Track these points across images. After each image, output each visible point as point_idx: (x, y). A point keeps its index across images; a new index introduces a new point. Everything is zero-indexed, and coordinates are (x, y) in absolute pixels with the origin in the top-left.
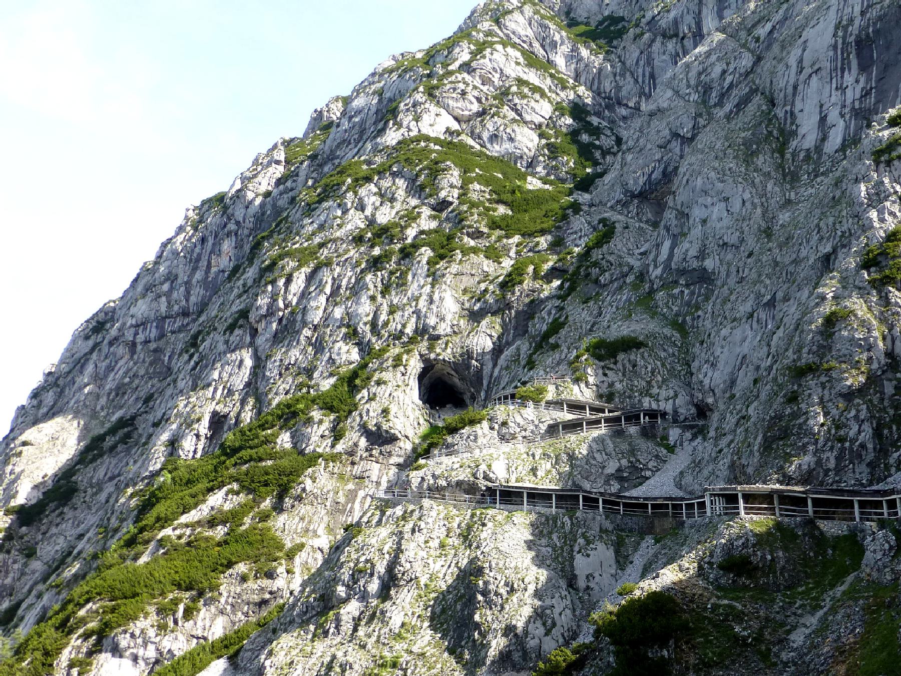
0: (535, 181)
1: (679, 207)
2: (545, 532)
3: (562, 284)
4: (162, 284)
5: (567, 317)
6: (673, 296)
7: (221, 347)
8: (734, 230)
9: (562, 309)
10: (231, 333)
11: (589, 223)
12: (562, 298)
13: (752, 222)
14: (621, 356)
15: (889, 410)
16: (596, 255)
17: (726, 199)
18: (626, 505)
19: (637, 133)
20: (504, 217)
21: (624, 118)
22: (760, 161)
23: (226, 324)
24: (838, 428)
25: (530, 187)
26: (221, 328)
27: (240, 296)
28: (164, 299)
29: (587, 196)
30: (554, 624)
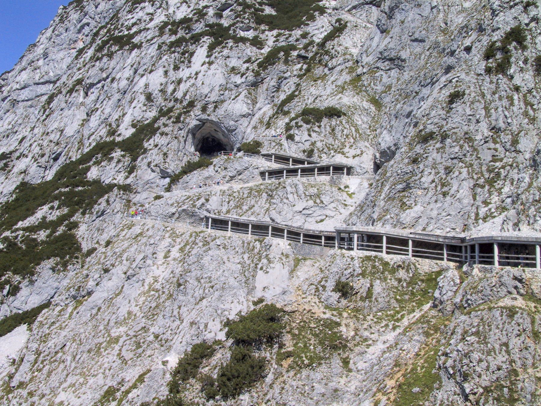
4: (38, 60)
5: (300, 91)
8: (421, 29)
10: (70, 95)
11: (329, 22)
15: (485, 173)
18: (305, 236)
20: (270, 16)
23: (68, 89)
24: (443, 185)
26: (64, 92)
27: (79, 69)
28: (38, 71)
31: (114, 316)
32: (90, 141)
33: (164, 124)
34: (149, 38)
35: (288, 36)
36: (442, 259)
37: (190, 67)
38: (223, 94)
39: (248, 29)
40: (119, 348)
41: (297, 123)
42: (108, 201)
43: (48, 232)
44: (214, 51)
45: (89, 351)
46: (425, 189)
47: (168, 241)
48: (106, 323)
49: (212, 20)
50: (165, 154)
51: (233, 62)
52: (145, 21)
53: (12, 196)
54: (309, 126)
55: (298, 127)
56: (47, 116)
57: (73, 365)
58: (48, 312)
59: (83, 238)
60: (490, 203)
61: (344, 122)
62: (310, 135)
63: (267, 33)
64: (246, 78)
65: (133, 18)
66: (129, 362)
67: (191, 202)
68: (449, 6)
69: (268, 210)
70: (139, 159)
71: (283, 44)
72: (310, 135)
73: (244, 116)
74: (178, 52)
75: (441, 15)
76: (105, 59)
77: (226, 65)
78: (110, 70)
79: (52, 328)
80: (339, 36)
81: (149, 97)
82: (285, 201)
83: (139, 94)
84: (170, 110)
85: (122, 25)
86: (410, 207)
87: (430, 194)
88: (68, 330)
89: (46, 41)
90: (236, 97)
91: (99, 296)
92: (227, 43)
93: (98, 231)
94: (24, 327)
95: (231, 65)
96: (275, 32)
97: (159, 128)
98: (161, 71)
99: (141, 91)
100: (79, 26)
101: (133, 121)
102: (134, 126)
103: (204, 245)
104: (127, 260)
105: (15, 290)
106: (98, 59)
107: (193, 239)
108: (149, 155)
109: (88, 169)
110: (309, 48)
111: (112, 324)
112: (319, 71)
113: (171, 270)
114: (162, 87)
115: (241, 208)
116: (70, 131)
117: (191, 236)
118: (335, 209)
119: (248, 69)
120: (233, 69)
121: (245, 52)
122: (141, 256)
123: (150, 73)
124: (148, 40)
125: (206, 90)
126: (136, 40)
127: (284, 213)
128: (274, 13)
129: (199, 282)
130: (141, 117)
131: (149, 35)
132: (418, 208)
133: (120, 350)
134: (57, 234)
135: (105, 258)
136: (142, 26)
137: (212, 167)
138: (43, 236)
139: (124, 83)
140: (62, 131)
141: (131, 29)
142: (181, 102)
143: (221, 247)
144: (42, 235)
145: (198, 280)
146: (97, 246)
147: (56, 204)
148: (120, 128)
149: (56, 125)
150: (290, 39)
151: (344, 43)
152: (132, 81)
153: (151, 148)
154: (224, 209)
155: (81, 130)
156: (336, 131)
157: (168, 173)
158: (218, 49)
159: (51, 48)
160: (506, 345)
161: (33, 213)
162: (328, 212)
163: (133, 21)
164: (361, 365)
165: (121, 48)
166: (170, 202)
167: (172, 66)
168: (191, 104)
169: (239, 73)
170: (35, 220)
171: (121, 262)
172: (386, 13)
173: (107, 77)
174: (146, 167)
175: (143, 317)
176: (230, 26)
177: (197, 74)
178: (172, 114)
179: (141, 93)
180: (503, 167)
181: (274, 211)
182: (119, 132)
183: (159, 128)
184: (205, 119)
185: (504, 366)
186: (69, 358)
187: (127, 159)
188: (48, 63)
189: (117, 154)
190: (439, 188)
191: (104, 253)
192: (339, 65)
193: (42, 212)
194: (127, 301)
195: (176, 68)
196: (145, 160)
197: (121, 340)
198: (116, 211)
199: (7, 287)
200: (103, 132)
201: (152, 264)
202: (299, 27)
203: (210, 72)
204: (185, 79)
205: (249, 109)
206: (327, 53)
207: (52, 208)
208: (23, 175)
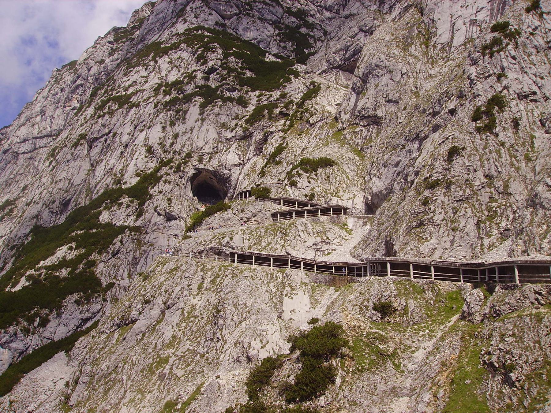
0: (270, 57)
1: (361, 76)
2: (265, 282)
3: (285, 122)
5: (287, 144)
6: (355, 133)
7: (69, 157)
8: (395, 92)
9: (285, 138)
10: (76, 148)
11: (304, 84)
12: (285, 131)
13: (407, 88)
14: (320, 171)
16: (308, 104)
17: (391, 72)
19: (337, 29)
20: (251, 78)
21: (330, 19)
22: (412, 49)
23: (73, 143)
24: (452, 222)
25: (268, 60)
26: (69, 145)
27: (82, 125)
29: (304, 67)
30: (267, 343)
31: (160, 340)
32: (97, 188)
33: (166, 173)
34: (145, 98)
35: (268, 96)
36: (460, 281)
37: (185, 123)
38: (217, 147)
39: (233, 90)
40: (170, 367)
41: (297, 172)
42: (121, 241)
43: (69, 269)
44: (206, 109)
45: (142, 371)
46: (437, 225)
47: (200, 274)
48: (153, 346)
49: (201, 83)
50: (169, 200)
51: (224, 118)
52: (140, 83)
53: (27, 239)
54: (308, 175)
55: (300, 175)
56: (54, 167)
57: (129, 383)
58: (84, 339)
59: (102, 275)
60: (492, 235)
61: (336, 169)
62: (309, 182)
63: (250, 93)
64: (236, 132)
65: (129, 80)
66: (182, 378)
67: (217, 241)
68: (417, 73)
69: (283, 245)
70: (146, 204)
71: (265, 103)
72: (309, 182)
73: (236, 165)
74: (173, 110)
75: (411, 80)
76: (107, 117)
77: (217, 122)
78: (112, 126)
79: (102, 353)
80: (315, 97)
81: (150, 150)
82: (298, 238)
83: (139, 147)
84: (170, 161)
85: (119, 86)
86: (427, 240)
87: (442, 230)
88: (118, 354)
89: (43, 100)
90: (227, 149)
91: (141, 325)
92: (217, 102)
93: (115, 267)
94: (62, 354)
95: (221, 122)
96: (257, 93)
97: (162, 176)
98: (159, 127)
99: (141, 144)
100: (73, 86)
101: (136, 171)
102: (137, 175)
103: (233, 277)
104: (166, 292)
105: (44, 323)
106: (99, 117)
107: (222, 272)
108: (155, 200)
109: (100, 213)
110: (290, 106)
111: (159, 346)
112: (298, 125)
113: (206, 299)
114: (161, 140)
115: (260, 245)
116: (78, 180)
117: (220, 270)
118: (338, 244)
119: (237, 125)
120: (224, 125)
121: (233, 110)
122: (179, 288)
123: (149, 128)
124: (145, 100)
125: (201, 144)
126: (134, 99)
127: (297, 248)
128: (254, 76)
129: (237, 308)
130: (144, 167)
131: (146, 95)
132: (434, 241)
133: (171, 369)
134: (77, 271)
135: (145, 291)
136: (138, 87)
137: (230, 211)
138: (65, 273)
139: (125, 138)
140: (70, 180)
141: (128, 90)
142: (180, 154)
143: (248, 278)
144: (64, 273)
145: (235, 306)
146: (114, 281)
147: (74, 245)
148: (126, 176)
149: (64, 175)
150: (272, 99)
151: (321, 103)
152: (133, 136)
153: (156, 194)
154: (246, 245)
155: (88, 179)
156: (331, 179)
157: (173, 215)
158: (209, 107)
159: (48, 106)
160: (539, 342)
161: (53, 254)
162: (334, 247)
163: (130, 82)
164: (410, 367)
165: (120, 107)
166: (199, 241)
167: (168, 123)
168: (189, 156)
169: (229, 128)
170: (56, 259)
171: (160, 294)
172: (360, 78)
173: (110, 132)
174: (153, 211)
175: (187, 340)
176: (217, 88)
177: (192, 129)
178: (172, 164)
179: (142, 146)
180: (499, 207)
181: (289, 247)
182: (124, 181)
183: (162, 176)
184: (201, 169)
185: (540, 359)
186: (125, 378)
187: (135, 203)
188: (45, 119)
189: (125, 199)
190: (449, 224)
191: (143, 286)
192: (319, 121)
193: (62, 252)
194: (171, 327)
195: (172, 124)
196: (151, 205)
197: (171, 360)
198: (129, 249)
199: (38, 319)
200: (109, 180)
201: (188, 295)
202: (279, 89)
203: (203, 128)
204: (181, 133)
205: (240, 159)
206: (307, 111)
207: (71, 248)
208: (35, 219)
